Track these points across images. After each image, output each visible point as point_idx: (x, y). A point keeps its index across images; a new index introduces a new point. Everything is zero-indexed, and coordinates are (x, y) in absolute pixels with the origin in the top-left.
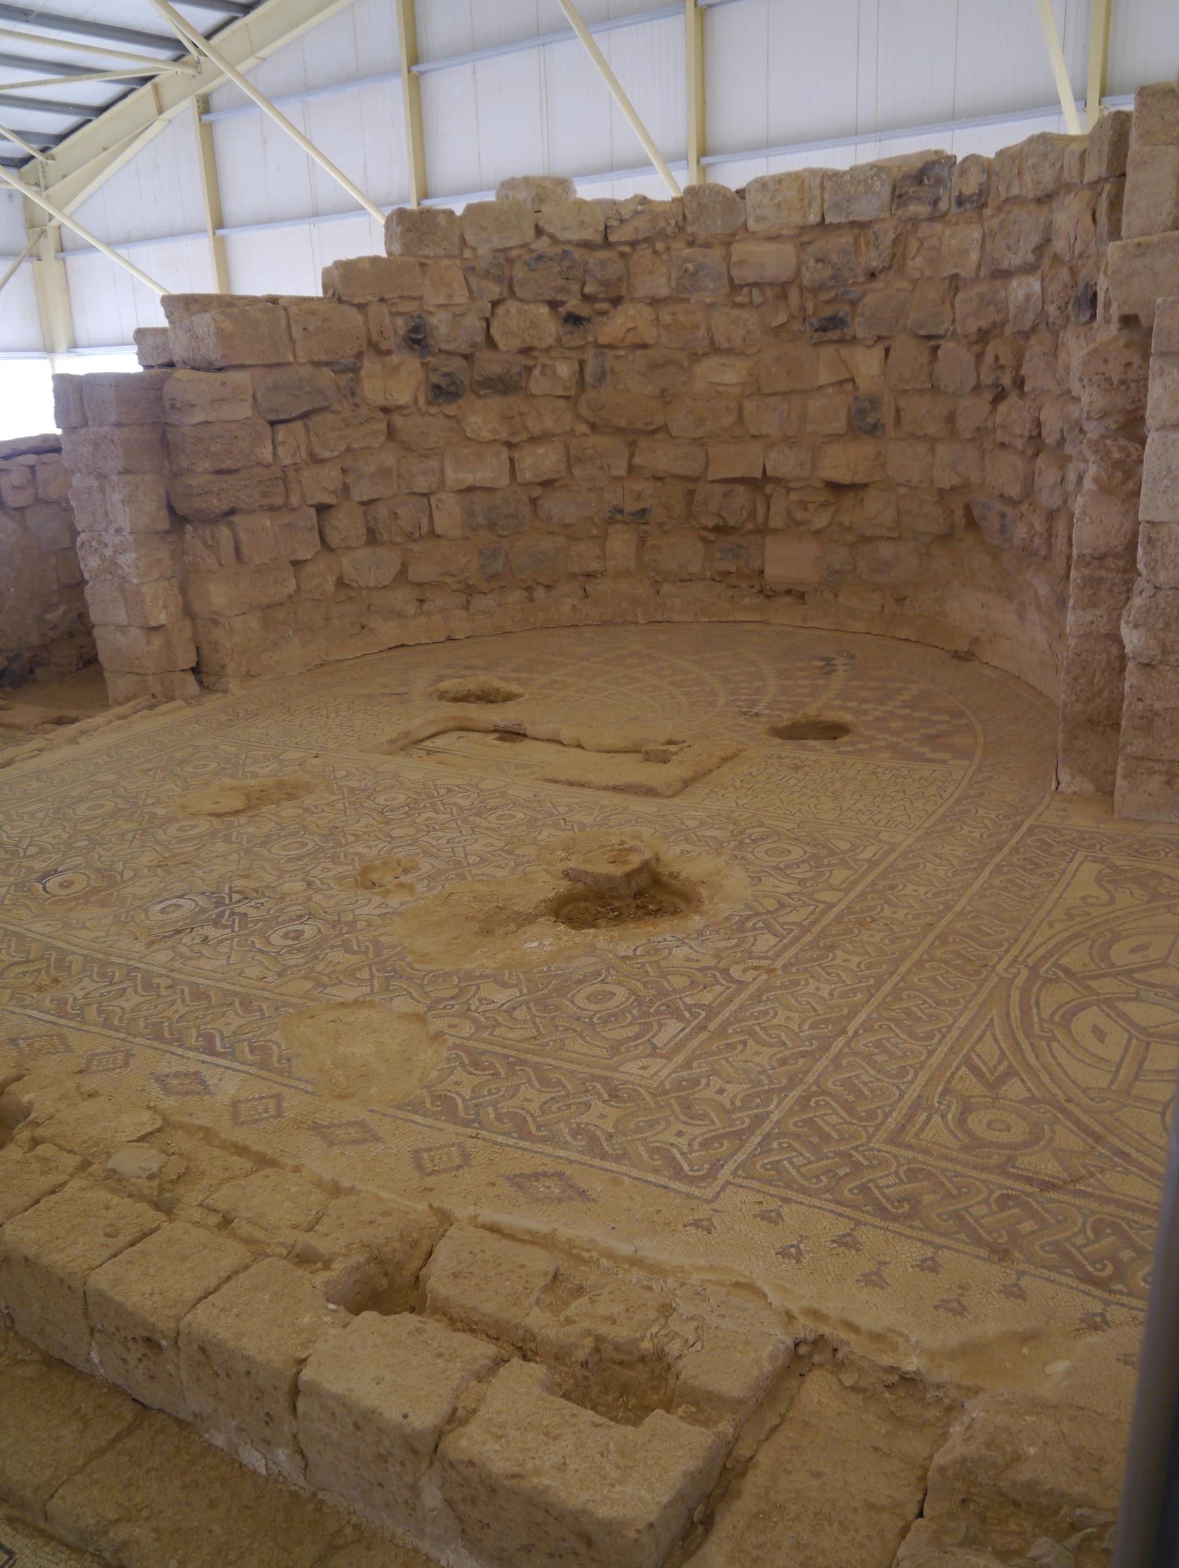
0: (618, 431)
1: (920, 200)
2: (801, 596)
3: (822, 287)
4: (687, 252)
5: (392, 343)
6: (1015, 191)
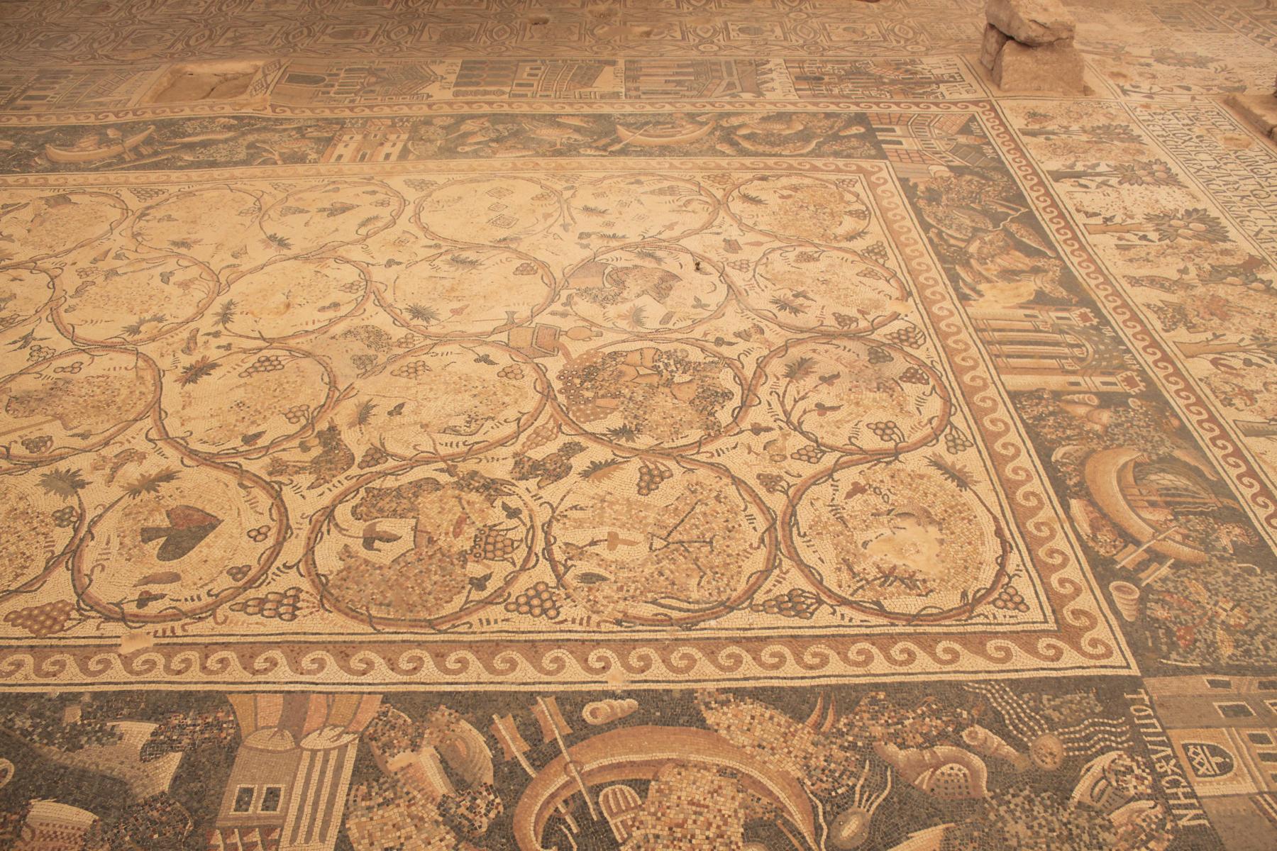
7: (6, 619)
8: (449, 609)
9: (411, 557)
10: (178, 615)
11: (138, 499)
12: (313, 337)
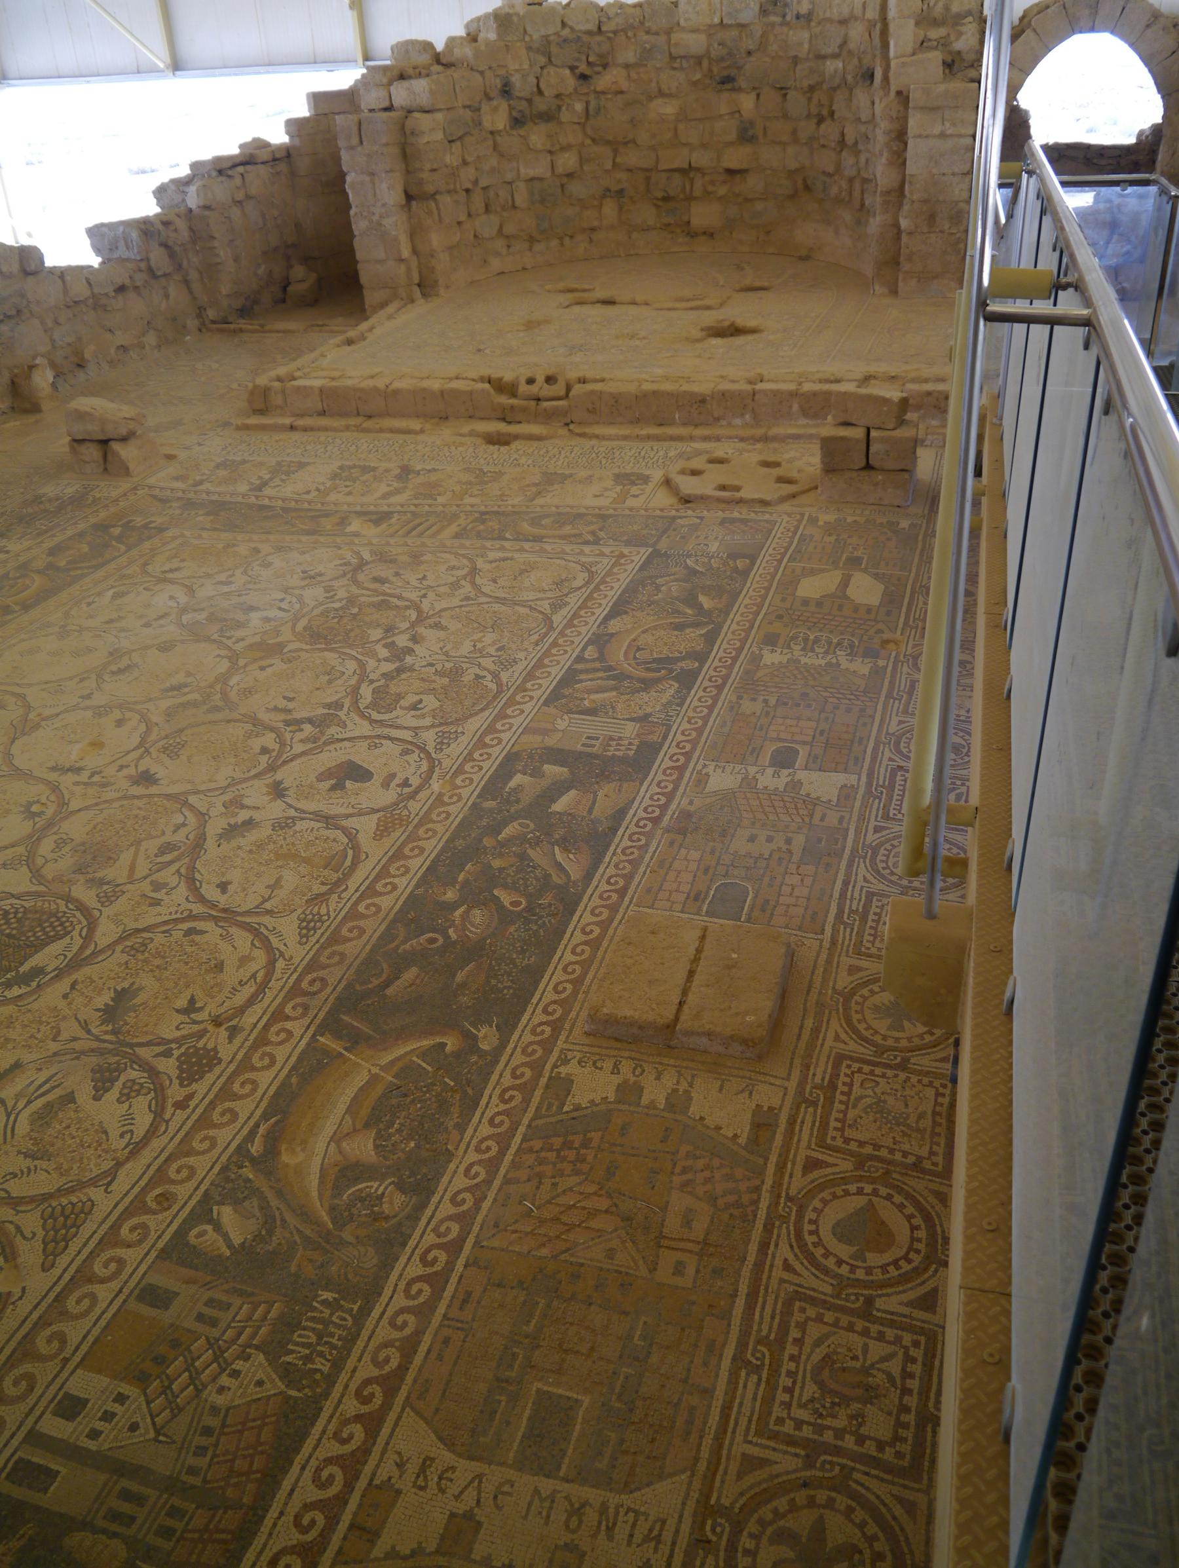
0: (608, 143)
1: (775, 14)
2: (712, 235)
3: (722, 59)
4: (645, 37)
5: (494, 93)
6: (828, 15)
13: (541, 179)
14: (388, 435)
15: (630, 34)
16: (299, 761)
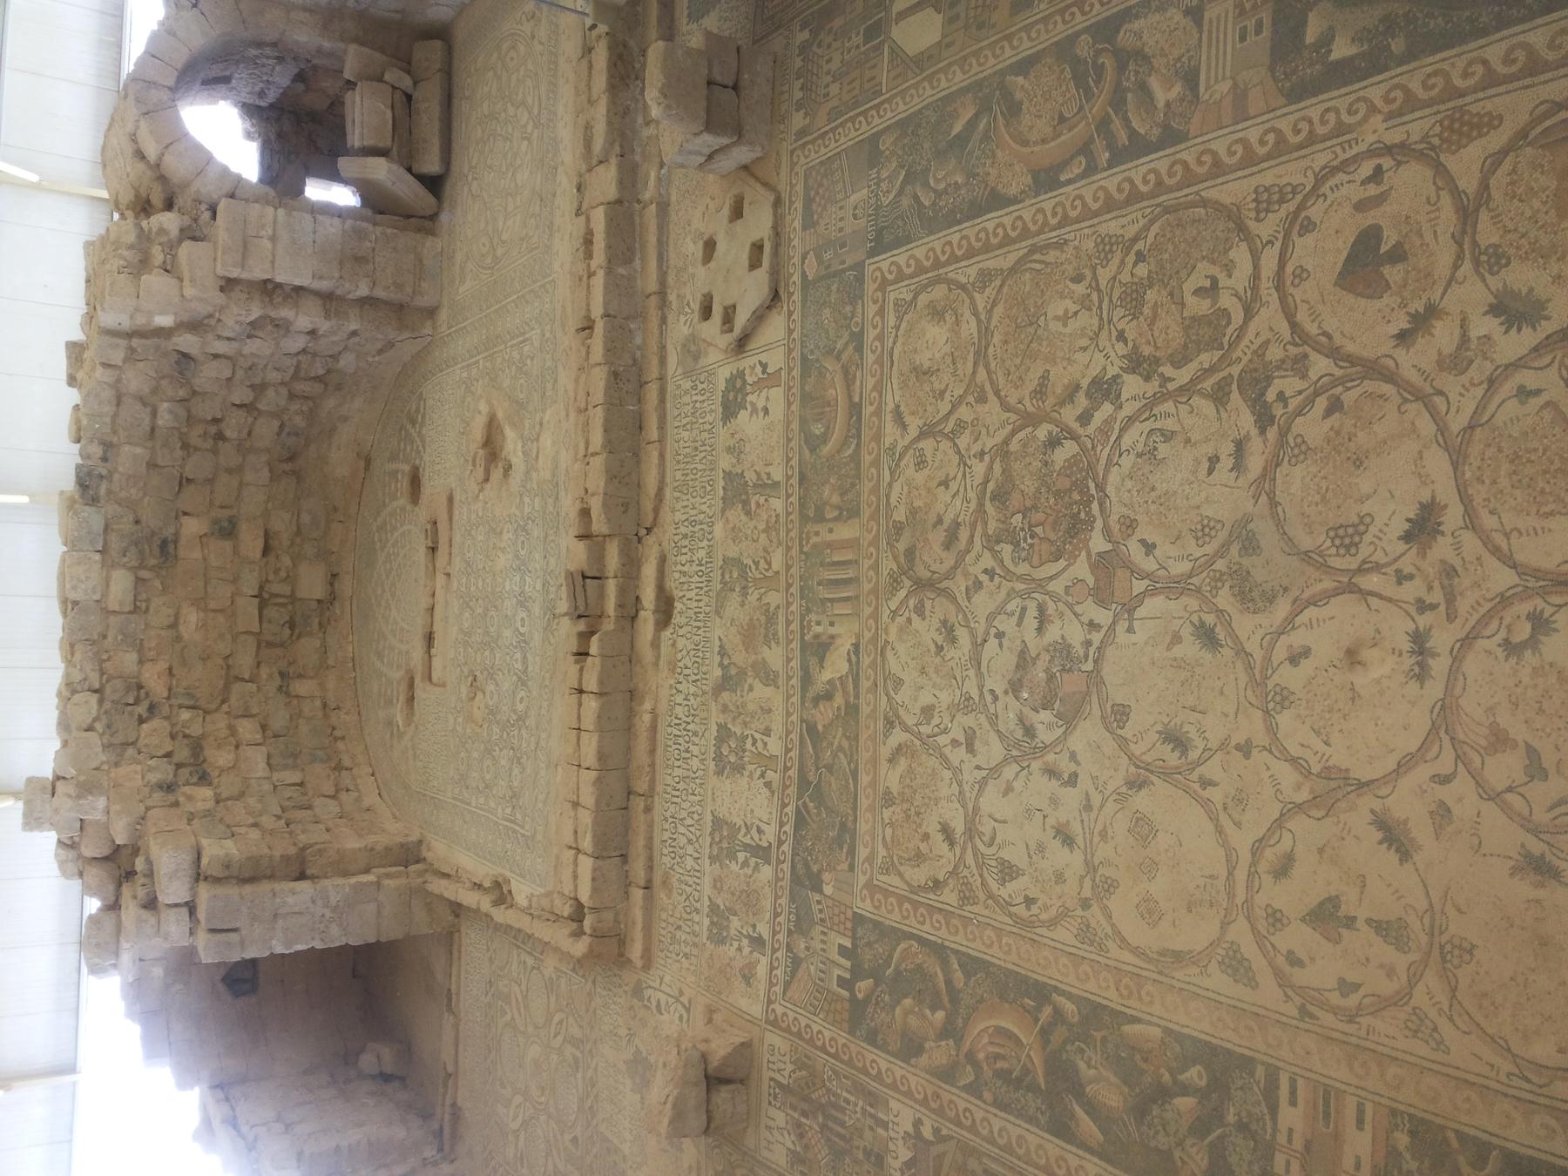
0: (227, 687)
3: (141, 552)
5: (171, 798)
6: (108, 420)
7: (1501, 118)
8: (1155, 229)
9: (1183, 274)
10: (1343, 167)
11: (1424, 300)
12: (1305, 596)
13: (269, 756)
14: (659, 751)
15: (105, 657)
16: (1350, 348)
